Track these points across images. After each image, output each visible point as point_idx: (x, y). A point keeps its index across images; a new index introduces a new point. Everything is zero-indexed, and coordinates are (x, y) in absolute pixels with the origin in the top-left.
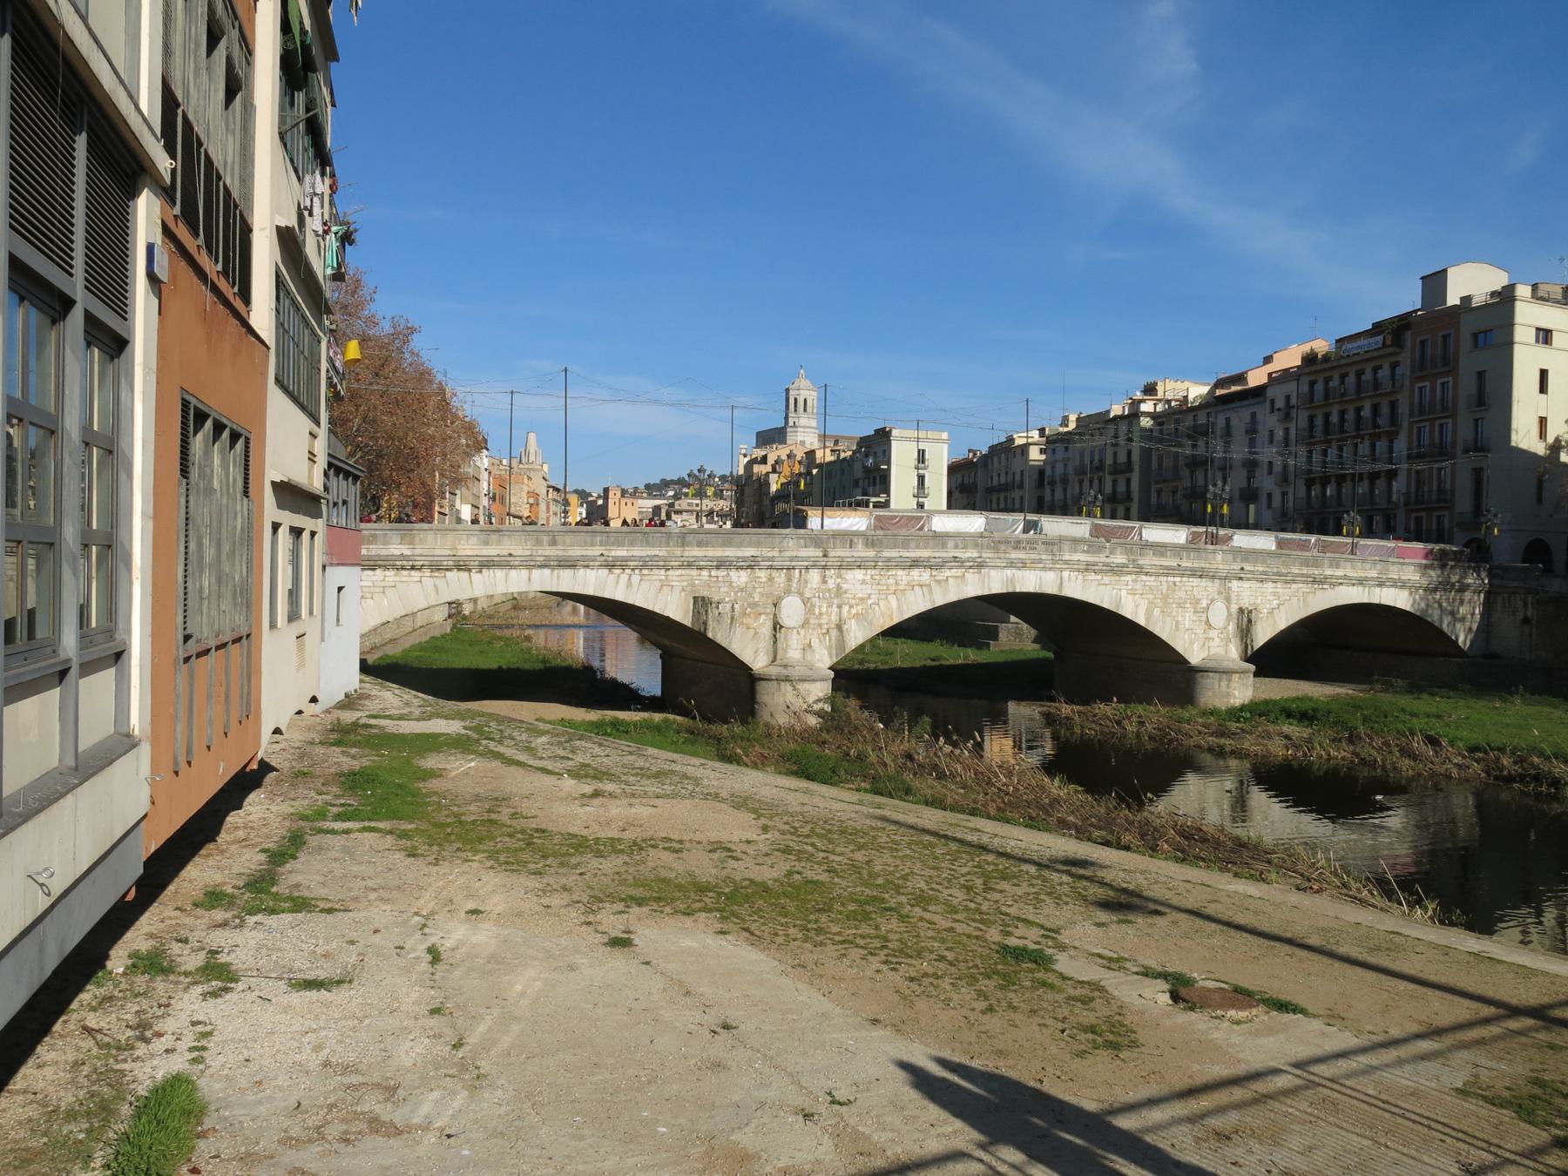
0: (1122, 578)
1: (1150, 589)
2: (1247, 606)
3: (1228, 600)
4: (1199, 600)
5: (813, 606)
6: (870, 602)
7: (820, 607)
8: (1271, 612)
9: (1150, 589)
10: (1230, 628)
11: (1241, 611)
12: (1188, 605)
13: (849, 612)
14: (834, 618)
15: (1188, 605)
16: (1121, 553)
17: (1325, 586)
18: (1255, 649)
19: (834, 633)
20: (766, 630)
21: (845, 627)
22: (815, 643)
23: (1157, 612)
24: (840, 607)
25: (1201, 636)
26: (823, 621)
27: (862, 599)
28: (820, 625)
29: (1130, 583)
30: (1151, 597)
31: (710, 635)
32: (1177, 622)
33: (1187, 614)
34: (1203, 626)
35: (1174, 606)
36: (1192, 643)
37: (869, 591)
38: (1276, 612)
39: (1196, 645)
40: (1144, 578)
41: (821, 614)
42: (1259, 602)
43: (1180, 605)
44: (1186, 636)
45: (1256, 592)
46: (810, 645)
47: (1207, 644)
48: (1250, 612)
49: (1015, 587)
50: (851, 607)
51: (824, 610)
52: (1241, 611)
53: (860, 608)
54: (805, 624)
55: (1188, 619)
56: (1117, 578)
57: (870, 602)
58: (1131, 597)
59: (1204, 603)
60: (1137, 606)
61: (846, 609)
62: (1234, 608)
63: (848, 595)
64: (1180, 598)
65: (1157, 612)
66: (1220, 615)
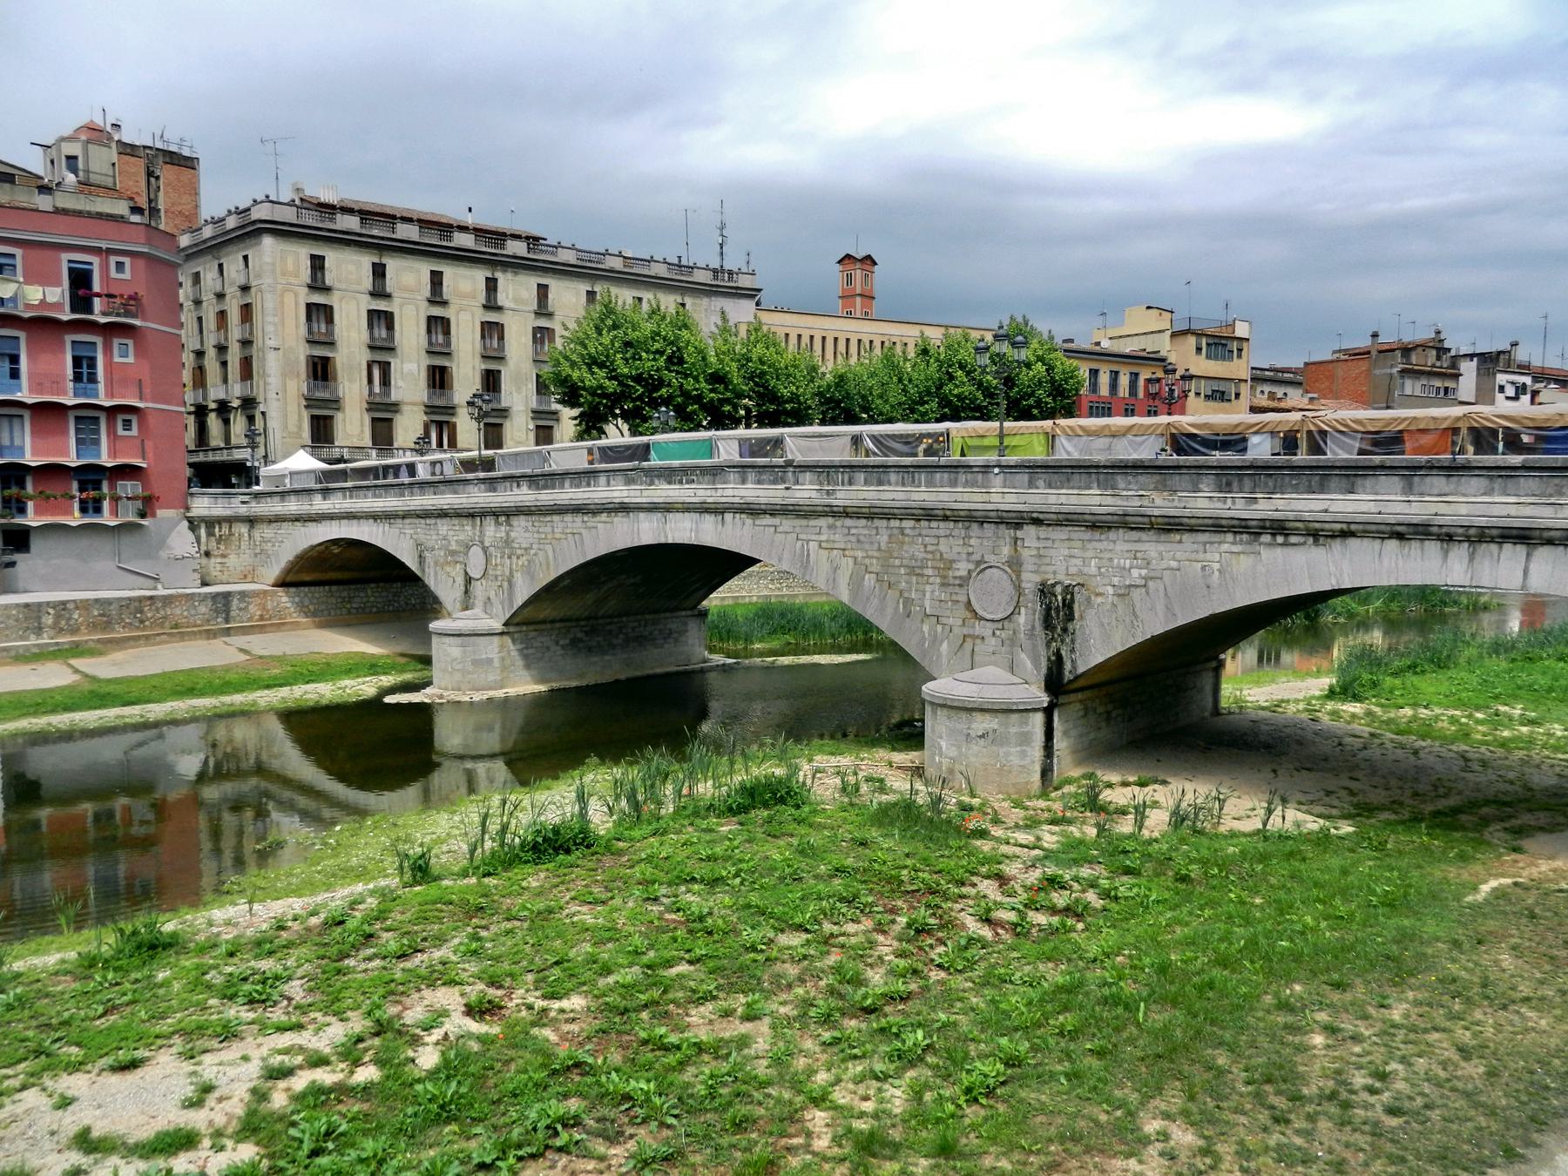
0: (812, 522)
1: (858, 541)
2: (1060, 577)
3: (1015, 564)
6: (532, 552)
8: (1124, 593)
9: (858, 541)
10: (1022, 619)
11: (1045, 591)
12: (930, 572)
13: (517, 564)
15: (930, 572)
16: (811, 483)
17: (1293, 539)
18: (1081, 670)
19: (506, 584)
20: (460, 580)
24: (509, 557)
25: (956, 630)
26: (498, 573)
27: (526, 549)
28: (496, 577)
29: (824, 530)
30: (860, 554)
32: (908, 602)
33: (928, 588)
34: (962, 612)
35: (903, 571)
36: (935, 641)
37: (531, 540)
38: (1137, 594)
39: (945, 645)
40: (849, 522)
42: (1093, 570)
43: (912, 571)
44: (926, 628)
45: (1084, 549)
47: (968, 646)
48: (1068, 590)
49: (666, 537)
52: (1045, 591)
55: (930, 595)
56: (804, 522)
57: (532, 552)
58: (825, 553)
59: (962, 568)
60: (836, 569)
61: (514, 558)
62: (1030, 580)
64: (912, 558)
66: (993, 594)
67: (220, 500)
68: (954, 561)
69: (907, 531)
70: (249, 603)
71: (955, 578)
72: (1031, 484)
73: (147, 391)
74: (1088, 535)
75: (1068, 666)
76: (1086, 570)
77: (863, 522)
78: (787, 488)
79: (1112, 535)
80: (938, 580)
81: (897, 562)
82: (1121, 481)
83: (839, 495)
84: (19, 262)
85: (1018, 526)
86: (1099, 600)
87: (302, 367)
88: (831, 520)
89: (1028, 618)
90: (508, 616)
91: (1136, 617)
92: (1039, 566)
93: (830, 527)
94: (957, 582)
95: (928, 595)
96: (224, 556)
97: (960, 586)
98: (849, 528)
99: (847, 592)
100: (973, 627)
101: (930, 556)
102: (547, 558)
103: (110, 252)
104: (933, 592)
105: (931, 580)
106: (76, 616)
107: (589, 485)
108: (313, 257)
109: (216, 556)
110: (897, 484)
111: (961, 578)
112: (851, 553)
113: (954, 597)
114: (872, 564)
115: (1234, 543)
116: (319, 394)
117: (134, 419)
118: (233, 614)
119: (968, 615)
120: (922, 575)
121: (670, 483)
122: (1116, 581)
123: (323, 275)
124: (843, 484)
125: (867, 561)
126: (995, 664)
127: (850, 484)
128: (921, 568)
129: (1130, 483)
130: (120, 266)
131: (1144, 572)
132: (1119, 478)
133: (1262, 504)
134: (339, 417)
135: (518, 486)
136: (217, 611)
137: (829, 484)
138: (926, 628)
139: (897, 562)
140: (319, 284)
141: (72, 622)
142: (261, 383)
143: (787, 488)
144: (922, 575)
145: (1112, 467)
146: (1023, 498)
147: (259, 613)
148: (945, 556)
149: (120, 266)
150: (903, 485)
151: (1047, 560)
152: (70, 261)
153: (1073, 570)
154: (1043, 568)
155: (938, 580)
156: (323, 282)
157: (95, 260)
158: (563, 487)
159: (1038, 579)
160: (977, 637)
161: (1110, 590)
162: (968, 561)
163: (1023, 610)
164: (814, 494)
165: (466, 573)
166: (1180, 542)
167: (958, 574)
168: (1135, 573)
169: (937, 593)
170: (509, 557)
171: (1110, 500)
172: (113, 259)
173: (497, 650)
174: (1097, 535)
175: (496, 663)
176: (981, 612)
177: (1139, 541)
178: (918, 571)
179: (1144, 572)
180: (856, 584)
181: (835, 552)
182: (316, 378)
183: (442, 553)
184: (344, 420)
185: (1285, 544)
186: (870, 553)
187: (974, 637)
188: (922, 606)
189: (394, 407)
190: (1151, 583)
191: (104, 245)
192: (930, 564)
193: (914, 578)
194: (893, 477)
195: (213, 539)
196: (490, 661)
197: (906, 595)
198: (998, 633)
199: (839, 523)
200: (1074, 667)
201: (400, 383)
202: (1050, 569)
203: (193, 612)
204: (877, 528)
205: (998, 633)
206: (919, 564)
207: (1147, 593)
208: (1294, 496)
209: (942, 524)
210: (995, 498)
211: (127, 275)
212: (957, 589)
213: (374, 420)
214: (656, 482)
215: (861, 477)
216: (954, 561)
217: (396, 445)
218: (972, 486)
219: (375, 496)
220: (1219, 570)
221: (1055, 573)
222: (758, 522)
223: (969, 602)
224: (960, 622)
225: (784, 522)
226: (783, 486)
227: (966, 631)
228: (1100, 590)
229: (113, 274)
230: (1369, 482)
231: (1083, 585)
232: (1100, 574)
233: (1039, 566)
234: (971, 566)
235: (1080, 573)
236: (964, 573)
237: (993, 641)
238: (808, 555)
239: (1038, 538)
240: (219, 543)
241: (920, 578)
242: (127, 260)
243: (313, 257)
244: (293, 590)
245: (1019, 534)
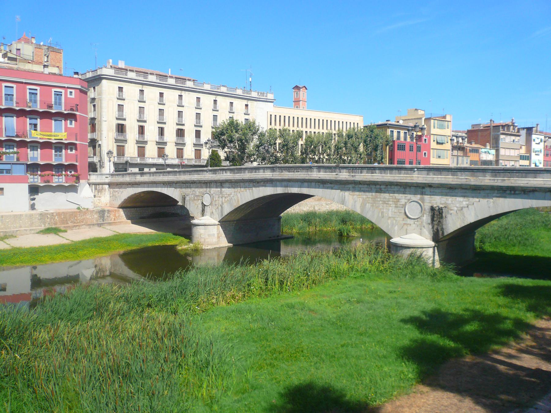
0: (346, 186)
4: (399, 199)
5: (214, 197)
6: (231, 196)
7: (216, 197)
11: (432, 209)
12: (391, 203)
14: (220, 203)
15: (391, 203)
16: (346, 173)
18: (445, 234)
19: (220, 207)
20: (200, 206)
21: (223, 206)
22: (214, 211)
23: (368, 206)
24: (222, 198)
26: (216, 203)
27: (229, 195)
28: (216, 205)
31: (186, 206)
33: (390, 208)
35: (381, 202)
37: (231, 192)
38: (465, 210)
39: (396, 228)
40: (360, 186)
41: (216, 200)
43: (384, 202)
46: (213, 212)
50: (225, 198)
51: (217, 199)
52: (432, 209)
53: (228, 198)
54: (211, 204)
56: (343, 186)
63: (223, 193)
65: (368, 206)
67: (99, 176)
68: (400, 199)
69: (383, 189)
70: (111, 214)
71: (400, 205)
72: (428, 174)
73: (78, 137)
74: (448, 191)
75: (440, 232)
76: (447, 202)
77: (366, 186)
78: (336, 174)
79: (456, 191)
80: (394, 205)
81: (379, 199)
82: (459, 173)
83: (357, 177)
84: (38, 92)
85: (423, 188)
86: (452, 212)
87: (114, 128)
88: (353, 185)
89: (427, 218)
90: (220, 219)
91: (465, 217)
92: (431, 201)
93: (353, 187)
94: (401, 206)
95: (390, 210)
96: (100, 197)
97: (402, 207)
98: (361, 188)
99: (360, 209)
100: (407, 221)
101: (391, 197)
102: (238, 197)
103: (68, 88)
104: (392, 209)
105: (391, 205)
106: (56, 218)
107: (256, 172)
108: (119, 87)
109: (97, 197)
110: (379, 173)
111: (402, 205)
112: (361, 196)
113: (400, 211)
114: (369, 200)
115: (498, 193)
116: (120, 138)
117: (74, 147)
118: (105, 218)
119: (405, 217)
120: (388, 204)
121: (289, 172)
122: (458, 205)
123: (122, 94)
124: (358, 173)
125: (367, 199)
126: (415, 233)
127: (361, 173)
128: (388, 201)
129: (462, 174)
130: (71, 92)
131: (467, 203)
132: (459, 172)
133: (506, 182)
134: (126, 146)
135: (226, 172)
136: (100, 217)
137: (353, 173)
138: (389, 221)
139: (379, 199)
140: (121, 98)
141: (55, 220)
142: (99, 134)
143: (336, 174)
144: (388, 204)
145: (457, 169)
146: (425, 179)
147: (113, 218)
148: (397, 198)
149: (71, 92)
150: (381, 174)
151: (433, 199)
152: (55, 91)
153: (443, 202)
154: (433, 202)
155: (394, 205)
156: (122, 96)
157: (63, 91)
158: (245, 173)
159: (430, 205)
160: (408, 224)
161: (456, 209)
162: (405, 199)
163: (425, 215)
164: (347, 177)
165: (202, 203)
166: (480, 193)
167: (401, 203)
168: (464, 203)
169: (394, 210)
170: (222, 198)
171: (456, 180)
172: (69, 90)
173: (216, 231)
174: (451, 191)
175: (216, 236)
176: (410, 216)
177: (466, 193)
178: (387, 202)
179: (467, 203)
180: (363, 206)
181: (355, 196)
182: (119, 132)
183: (193, 196)
184: (128, 147)
185: (514, 194)
186: (368, 196)
187: (407, 224)
188: (388, 214)
189: (146, 142)
190: (470, 206)
191: (66, 85)
192: (391, 200)
193: (385, 205)
194: (377, 171)
195: (96, 191)
196: (214, 235)
197: (382, 210)
198: (416, 223)
199: (357, 186)
200: (443, 233)
201: (148, 134)
202: (435, 202)
203: (93, 217)
204: (371, 188)
205: (416, 223)
206: (387, 200)
207: (468, 209)
208: (517, 179)
209: (396, 187)
210: (415, 178)
211: (73, 96)
212: (401, 208)
213: (138, 147)
214: (284, 171)
215: (365, 171)
216: (400, 199)
217: (146, 156)
218: (407, 174)
219: (164, 176)
220: (493, 202)
221: (436, 203)
222: (325, 186)
223: (405, 213)
224: (402, 219)
225: (335, 186)
226: (335, 174)
227: (404, 222)
228: (452, 208)
229: (69, 96)
230: (541, 175)
231: (446, 207)
232: (452, 203)
233: (431, 201)
234: (406, 201)
235: (446, 203)
236: (403, 203)
237: (414, 225)
238: (345, 197)
239: (431, 192)
240: (98, 192)
241: (387, 205)
242: (73, 91)
243: (119, 87)
244: (125, 209)
245: (424, 190)
